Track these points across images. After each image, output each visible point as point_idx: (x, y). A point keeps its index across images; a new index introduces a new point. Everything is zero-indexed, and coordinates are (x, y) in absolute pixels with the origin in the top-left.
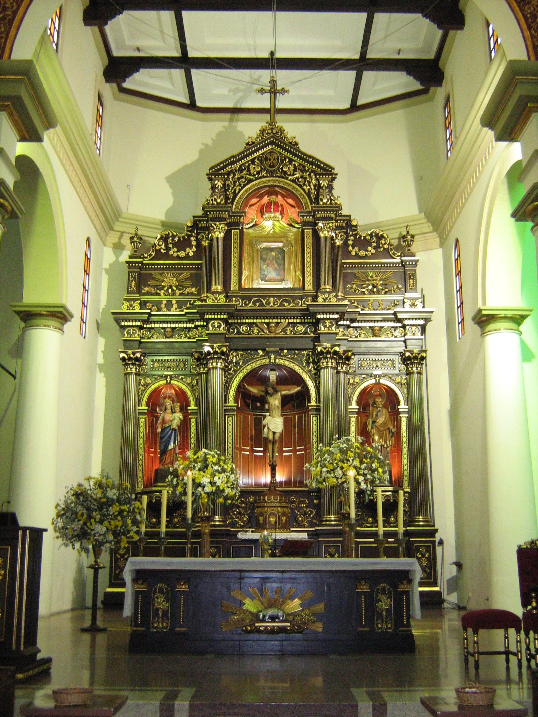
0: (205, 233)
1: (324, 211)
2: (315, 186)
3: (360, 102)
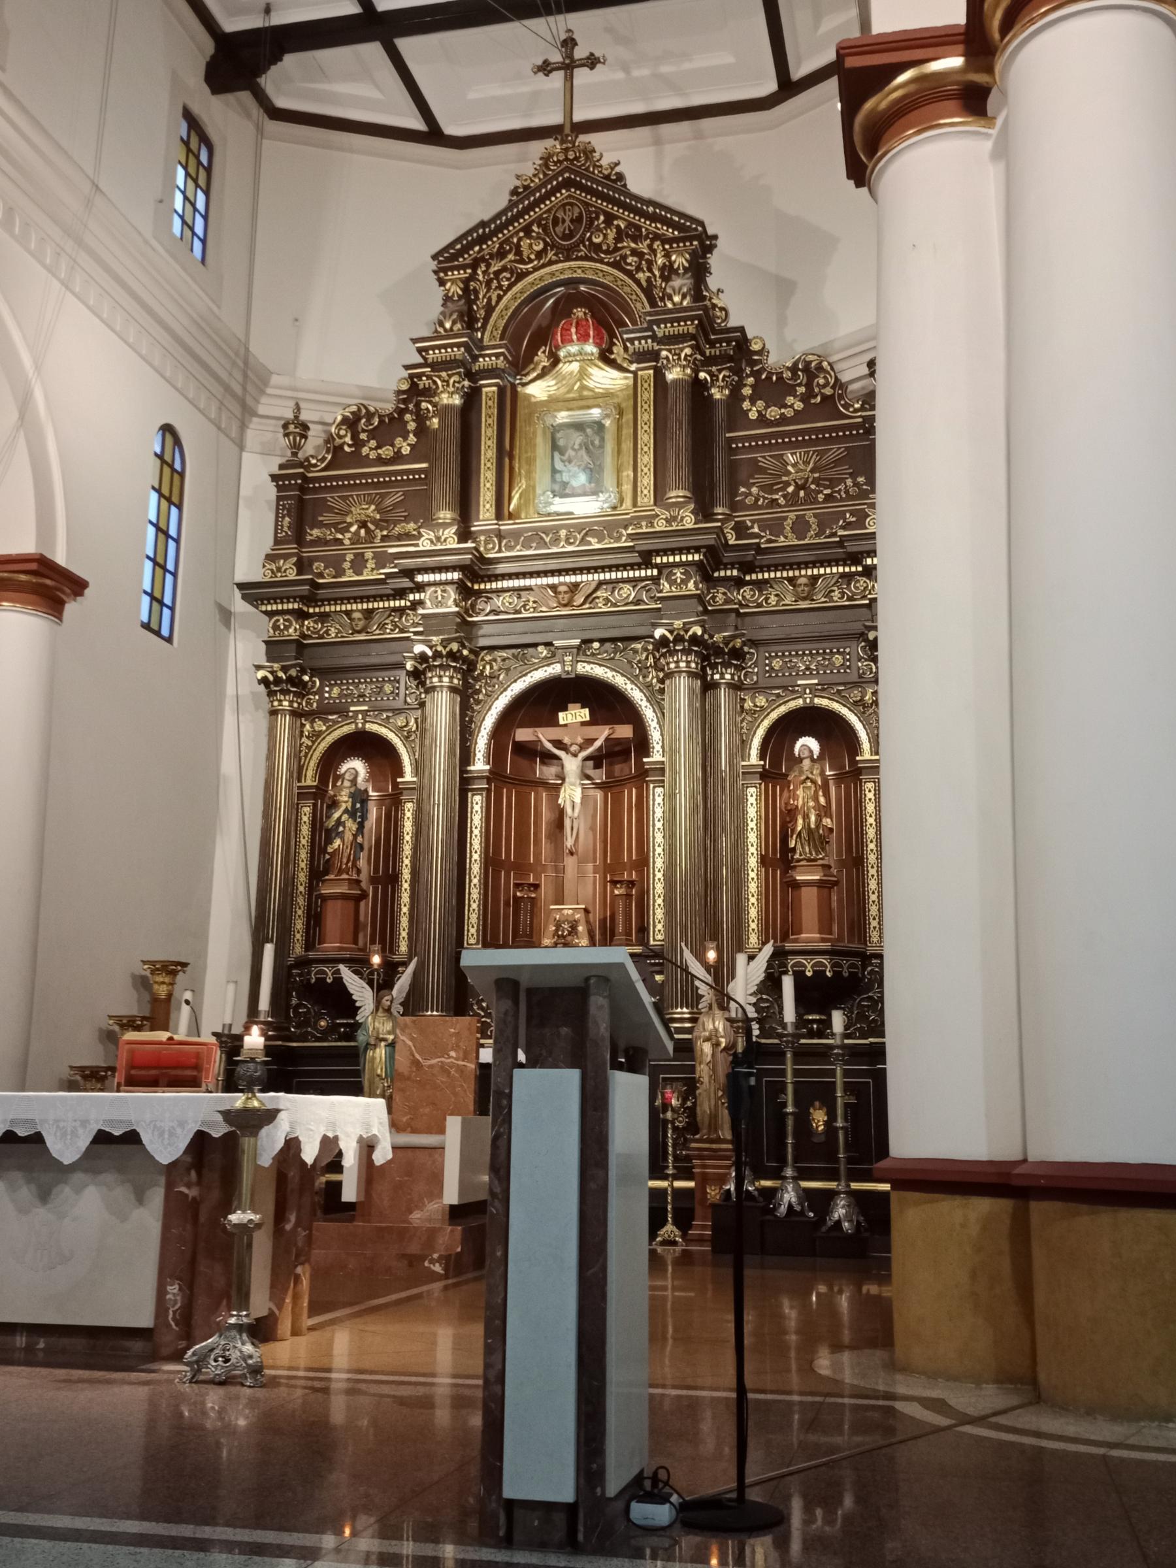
1: (672, 321)
2: (662, 269)
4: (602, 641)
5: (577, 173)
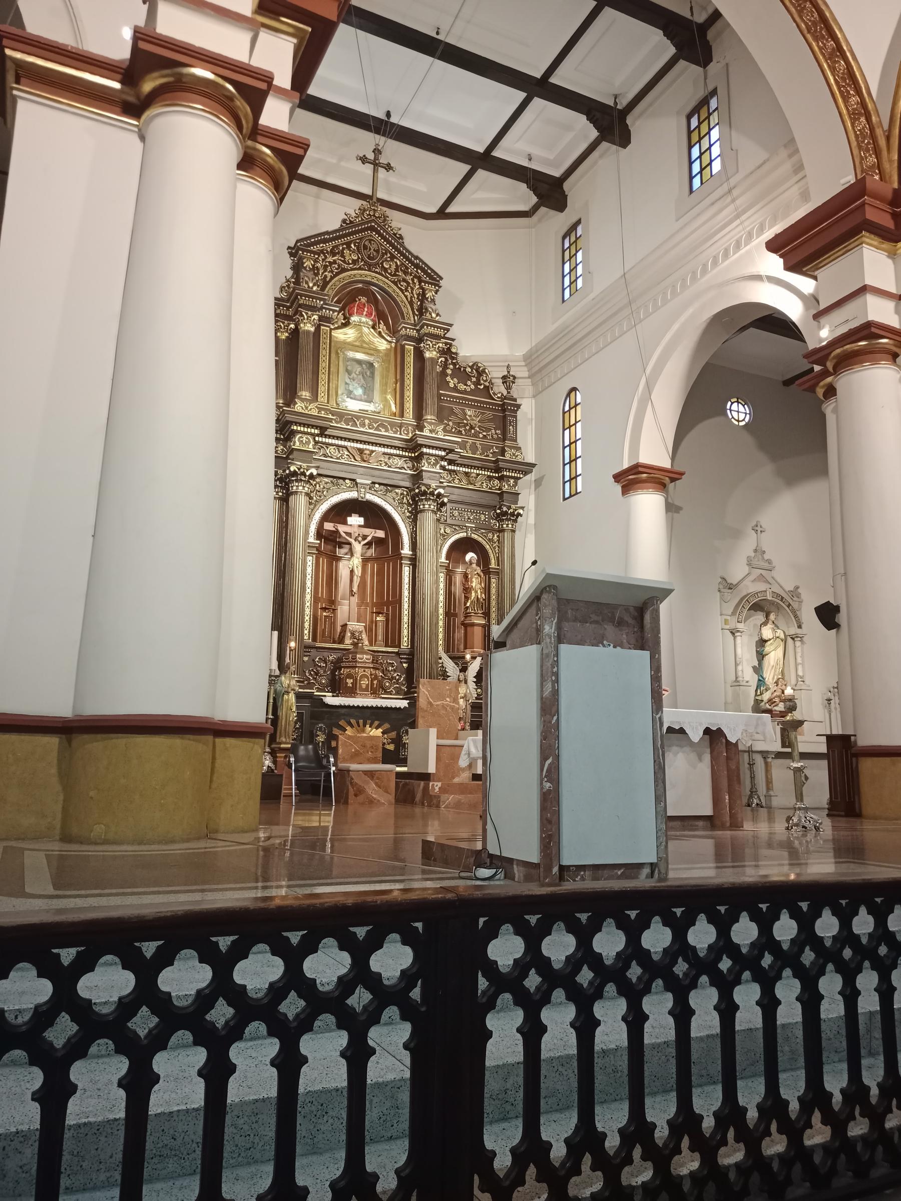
0: (283, 323)
3: (452, 209)
4: (380, 484)
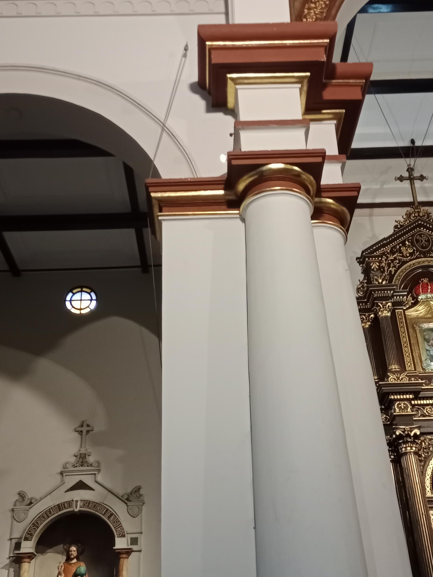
0: (365, 315)
5: (425, 222)
